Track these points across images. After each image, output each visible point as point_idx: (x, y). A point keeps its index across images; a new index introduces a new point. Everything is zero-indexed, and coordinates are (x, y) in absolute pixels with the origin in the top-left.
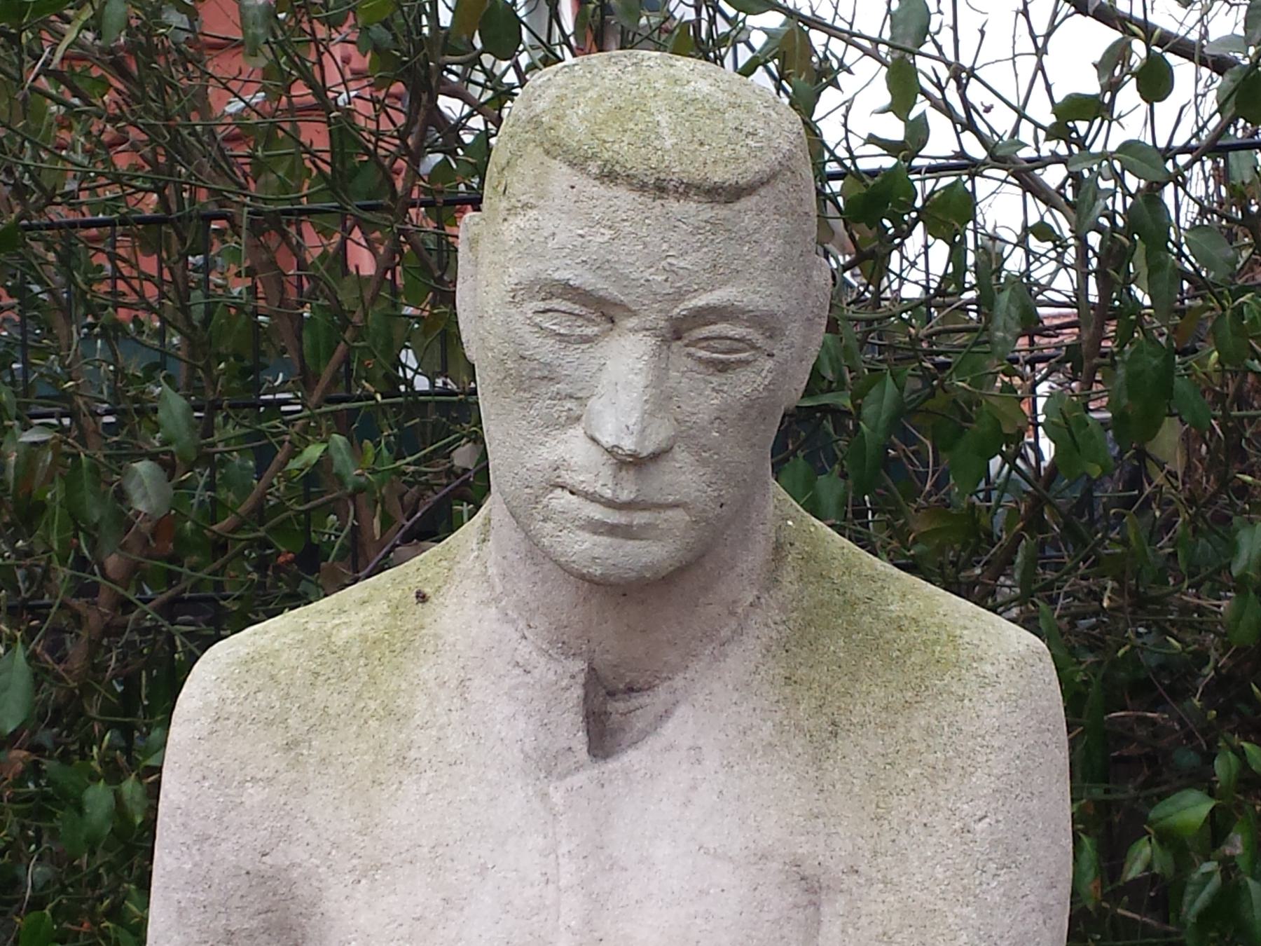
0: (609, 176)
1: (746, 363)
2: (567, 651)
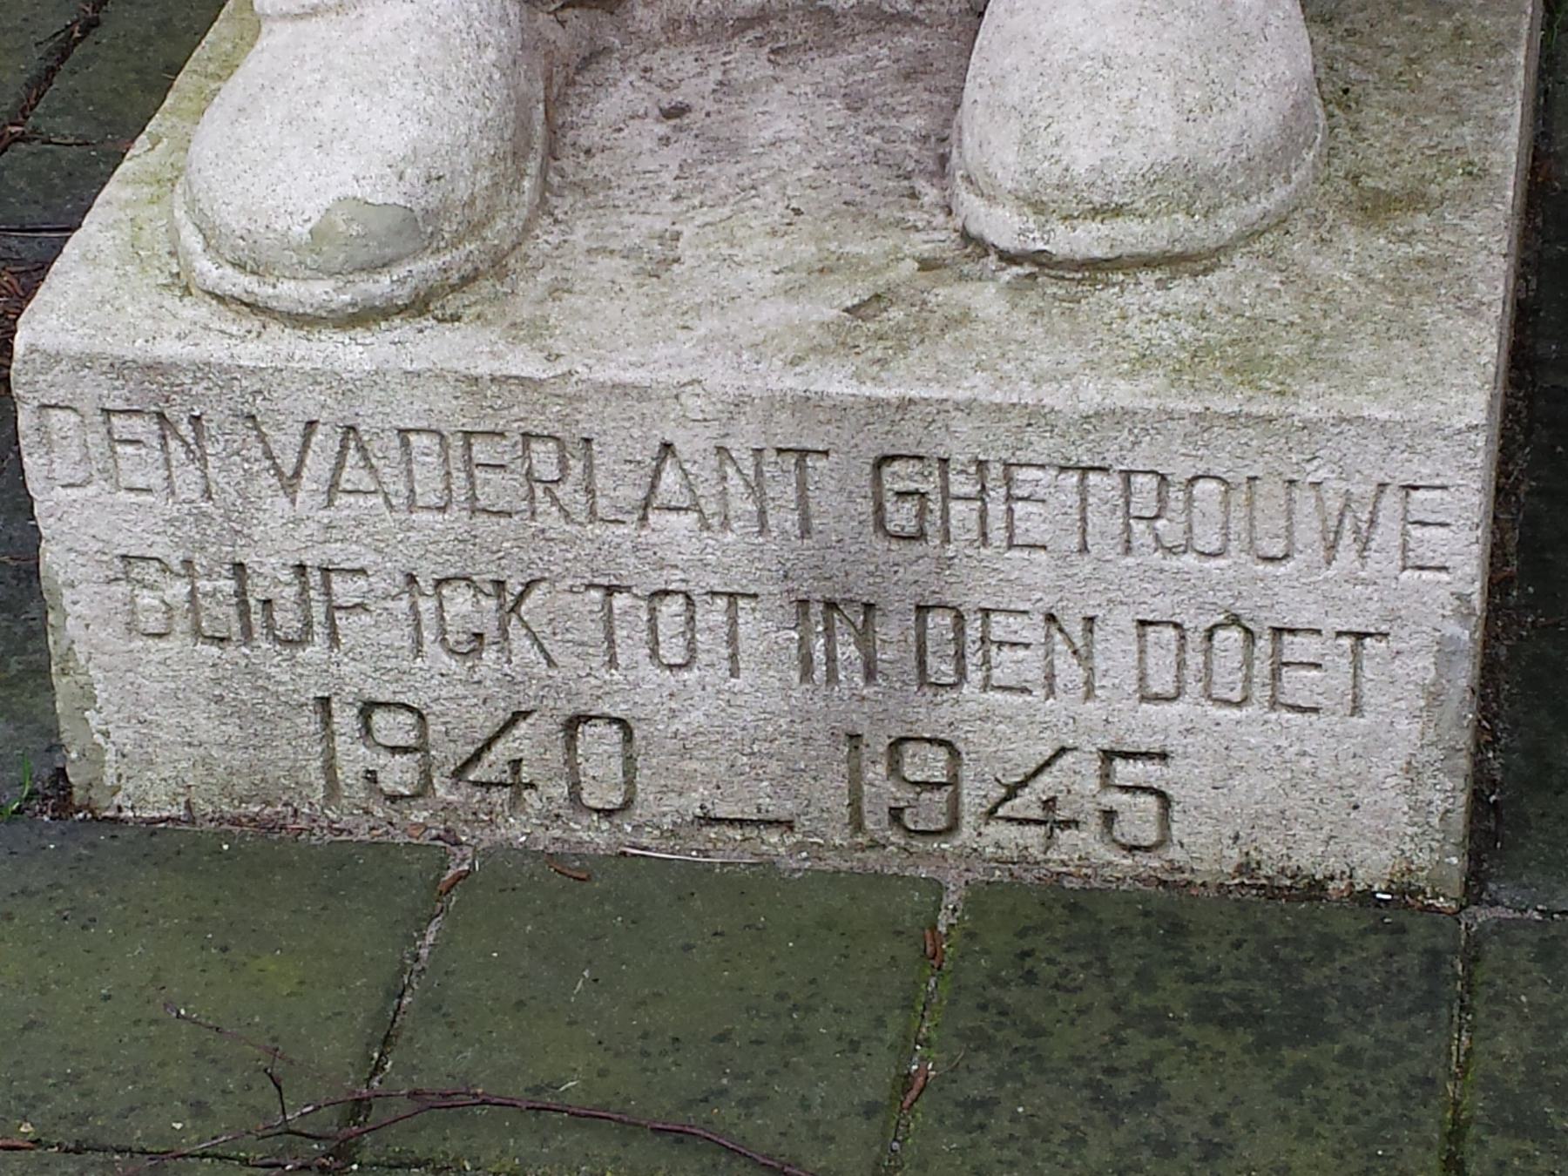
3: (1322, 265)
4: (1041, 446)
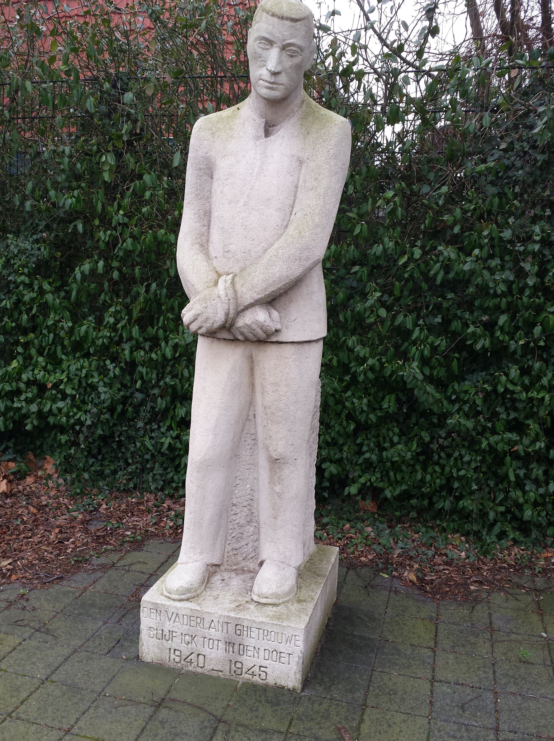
0: (273, 15)
1: (296, 56)
3: (292, 607)
4: (254, 625)
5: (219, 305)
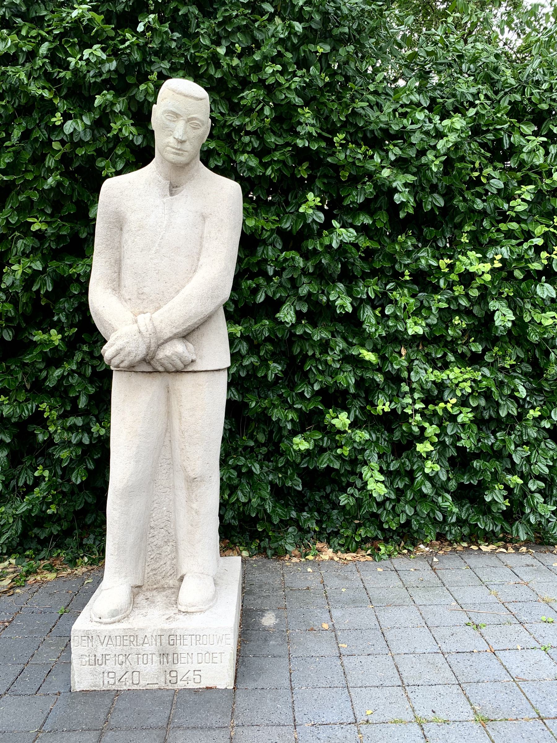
2: (166, 179)
5: (140, 339)
